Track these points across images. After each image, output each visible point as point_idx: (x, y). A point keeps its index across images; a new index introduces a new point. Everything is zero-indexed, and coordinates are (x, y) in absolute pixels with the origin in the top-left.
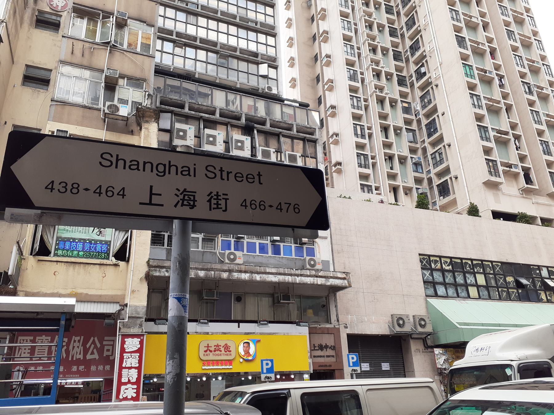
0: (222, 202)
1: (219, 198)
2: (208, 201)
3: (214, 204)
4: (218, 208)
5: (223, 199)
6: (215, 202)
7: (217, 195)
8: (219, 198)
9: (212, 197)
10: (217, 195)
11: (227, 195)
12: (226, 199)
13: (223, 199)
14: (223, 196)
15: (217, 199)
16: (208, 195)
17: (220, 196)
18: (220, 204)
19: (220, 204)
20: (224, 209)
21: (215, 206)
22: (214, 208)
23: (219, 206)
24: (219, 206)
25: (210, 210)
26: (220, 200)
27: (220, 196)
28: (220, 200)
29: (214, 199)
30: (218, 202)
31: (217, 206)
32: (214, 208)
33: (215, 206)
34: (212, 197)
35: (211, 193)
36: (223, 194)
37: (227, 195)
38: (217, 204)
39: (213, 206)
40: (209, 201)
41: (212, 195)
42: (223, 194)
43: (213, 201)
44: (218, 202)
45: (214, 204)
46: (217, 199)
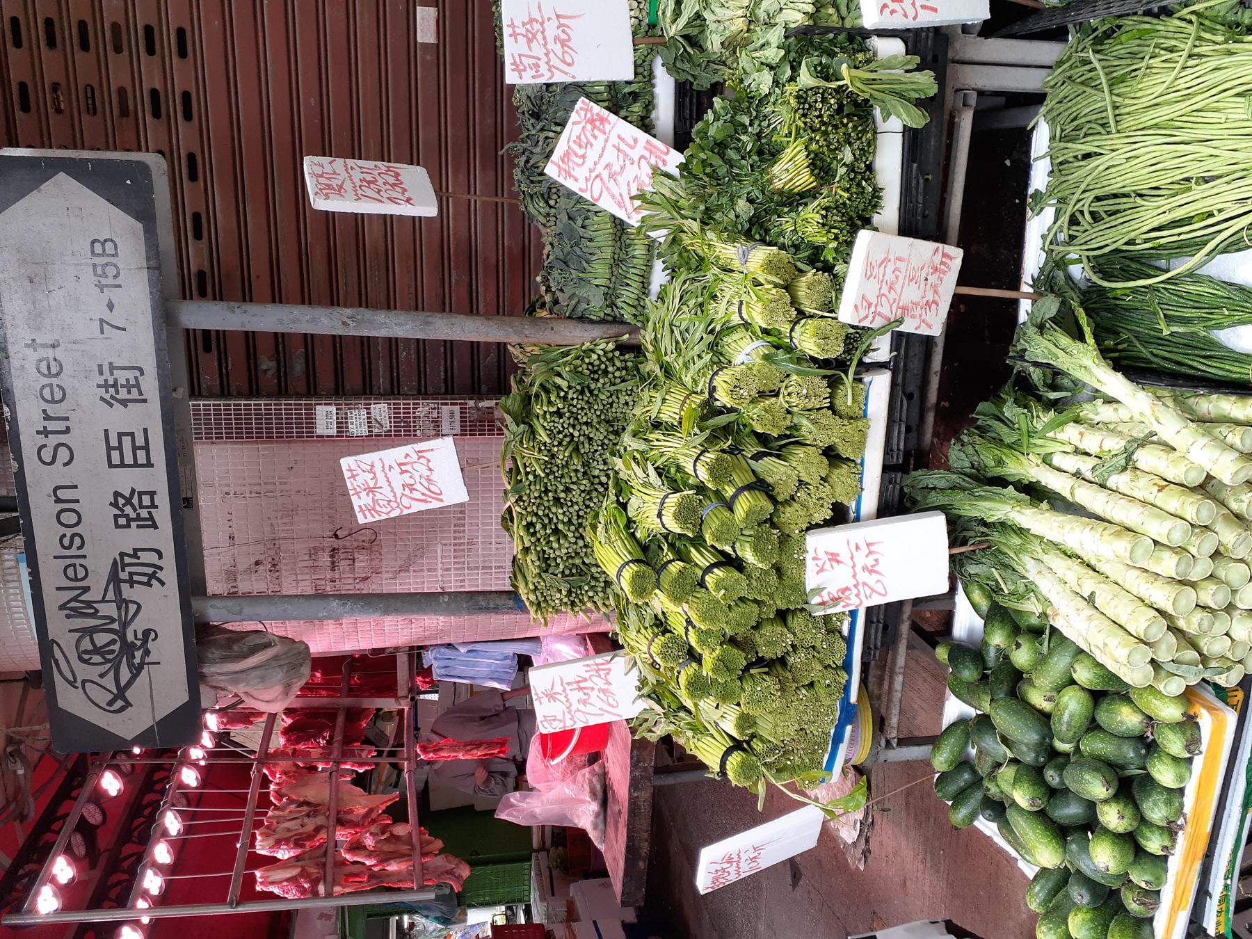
0: (122, 377)
1: (111, 382)
2: (126, 407)
3: (129, 392)
4: (137, 386)
5: (112, 374)
7: (106, 386)
9: (112, 397)
10: (106, 386)
11: (100, 366)
12: (112, 368)
13: (112, 374)
16: (111, 405)
17: (106, 381)
18: (128, 380)
19: (128, 380)
21: (134, 391)
22: (141, 394)
23: (132, 382)
24: (132, 382)
25: (145, 401)
26: (116, 381)
27: (106, 381)
28: (116, 381)
29: (117, 392)
30: (122, 386)
31: (133, 386)
32: (141, 394)
33: (134, 391)
36: (101, 373)
37: (100, 366)
38: (128, 386)
39: (135, 394)
40: (124, 403)
41: (107, 397)
42: (101, 373)
43: (123, 394)
44: (122, 386)
45: (129, 392)
46: (115, 385)
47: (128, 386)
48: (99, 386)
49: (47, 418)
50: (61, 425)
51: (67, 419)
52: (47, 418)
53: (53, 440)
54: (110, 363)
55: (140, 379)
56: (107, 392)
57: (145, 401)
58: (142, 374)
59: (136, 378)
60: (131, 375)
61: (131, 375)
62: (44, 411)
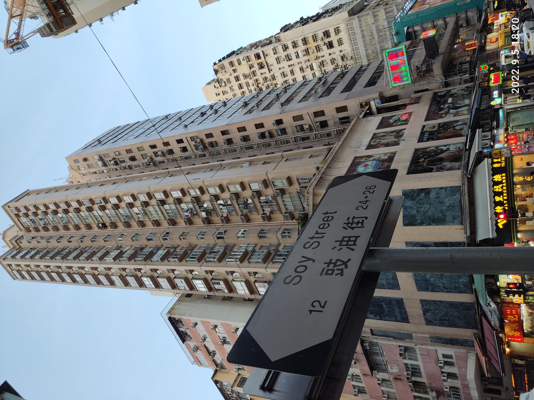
0: (356, 220)
1: (351, 222)
6: (354, 225)
9: (349, 227)
15: (352, 224)
16: (346, 229)
22: (362, 224)
26: (353, 222)
28: (353, 222)
34: (349, 227)
35: (344, 227)
38: (358, 222)
40: (353, 228)
41: (345, 226)
43: (354, 225)
49: (317, 233)
50: (321, 235)
51: (325, 233)
52: (317, 233)
53: (314, 240)
59: (363, 221)
62: (317, 232)
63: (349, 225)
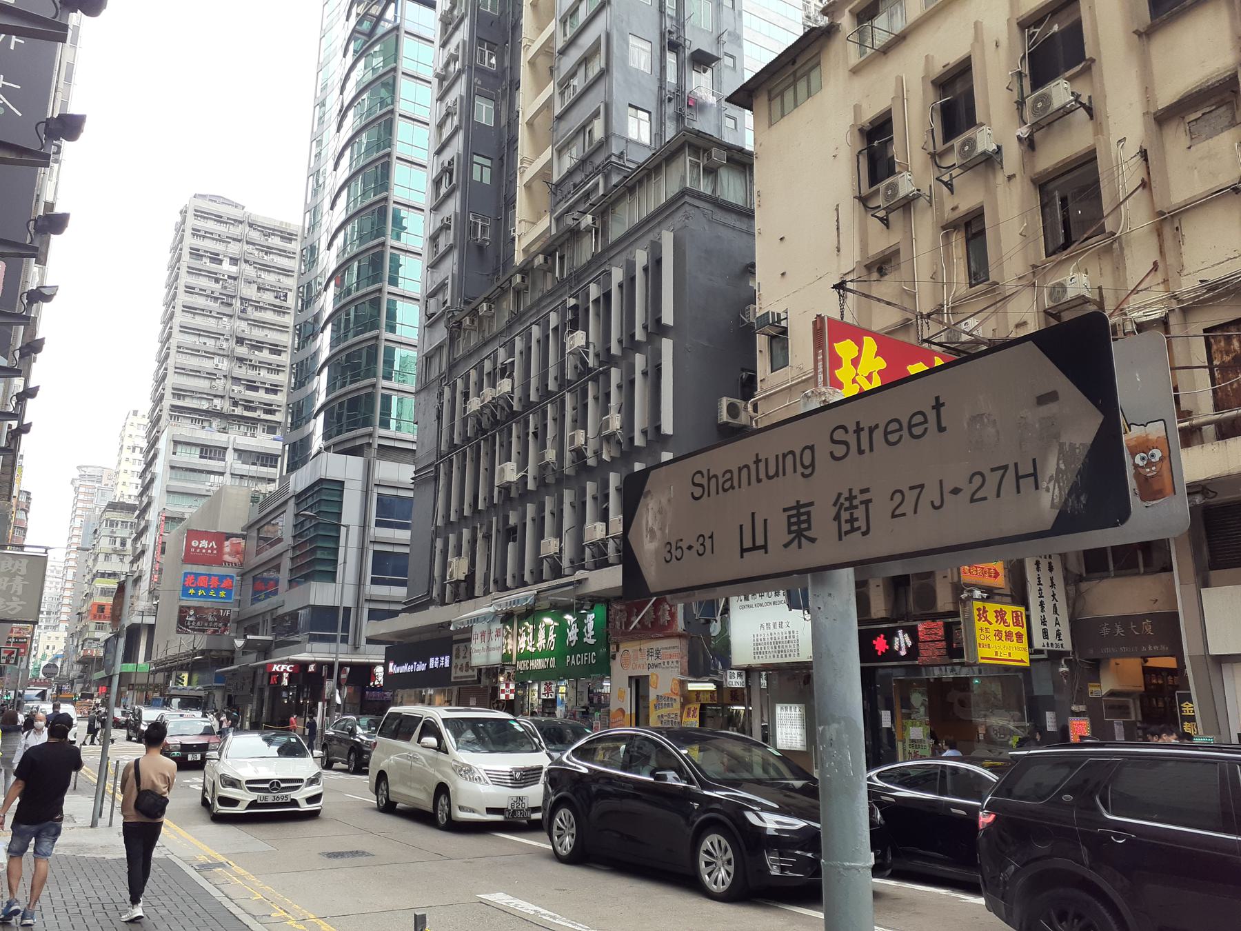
0: (859, 513)
3: (846, 521)
4: (853, 530)
5: (862, 503)
7: (851, 498)
8: (855, 502)
10: (851, 498)
12: (867, 503)
14: (861, 497)
16: (835, 505)
18: (857, 519)
19: (857, 519)
20: (864, 529)
22: (847, 533)
23: (856, 525)
24: (856, 525)
25: (840, 539)
26: (856, 507)
28: (856, 507)
29: (846, 509)
30: (852, 514)
32: (847, 533)
38: (852, 520)
40: (837, 517)
43: (845, 515)
44: (852, 514)
45: (846, 521)
47: (852, 520)
48: (850, 490)
54: (870, 501)
55: (858, 534)
56: (846, 499)
57: (840, 539)
58: (864, 534)
59: (859, 528)
60: (861, 523)
61: (861, 523)
63: (847, 504)
